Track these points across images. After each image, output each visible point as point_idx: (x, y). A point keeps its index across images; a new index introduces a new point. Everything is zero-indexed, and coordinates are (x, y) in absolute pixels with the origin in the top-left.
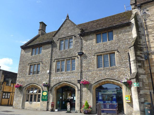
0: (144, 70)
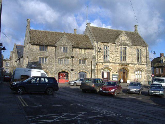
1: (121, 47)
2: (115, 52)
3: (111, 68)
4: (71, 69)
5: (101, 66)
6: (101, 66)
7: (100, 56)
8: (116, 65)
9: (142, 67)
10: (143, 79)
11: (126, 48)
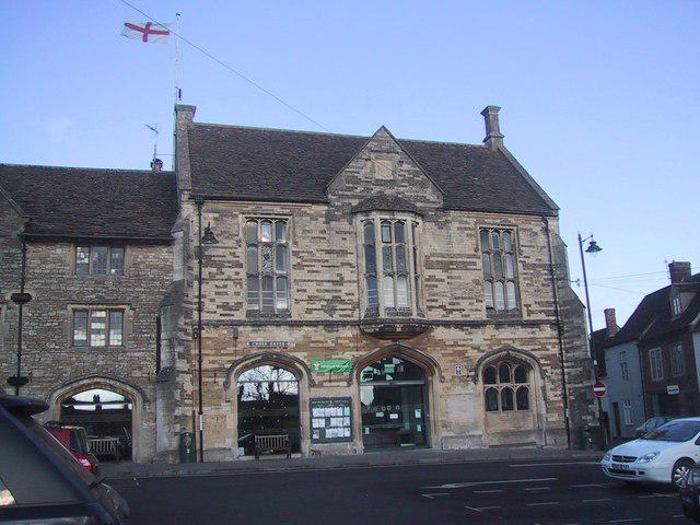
1: (369, 224)
2: (328, 252)
3: (301, 355)
4: (13, 373)
5: (230, 349)
6: (230, 349)
7: (221, 284)
8: (335, 335)
9: (524, 341)
10: (539, 416)
11: (401, 223)
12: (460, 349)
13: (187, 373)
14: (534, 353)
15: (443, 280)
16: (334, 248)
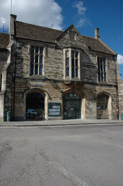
0: (10, 89)
2: (55, 59)
5: (24, 86)
6: (24, 86)
9: (108, 90)
12: (91, 90)
13: (10, 92)
14: (110, 93)
15: (87, 70)
16: (58, 58)
